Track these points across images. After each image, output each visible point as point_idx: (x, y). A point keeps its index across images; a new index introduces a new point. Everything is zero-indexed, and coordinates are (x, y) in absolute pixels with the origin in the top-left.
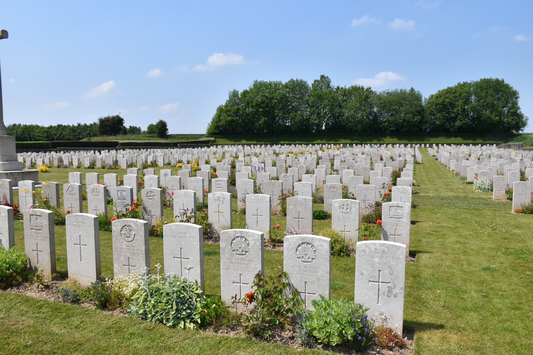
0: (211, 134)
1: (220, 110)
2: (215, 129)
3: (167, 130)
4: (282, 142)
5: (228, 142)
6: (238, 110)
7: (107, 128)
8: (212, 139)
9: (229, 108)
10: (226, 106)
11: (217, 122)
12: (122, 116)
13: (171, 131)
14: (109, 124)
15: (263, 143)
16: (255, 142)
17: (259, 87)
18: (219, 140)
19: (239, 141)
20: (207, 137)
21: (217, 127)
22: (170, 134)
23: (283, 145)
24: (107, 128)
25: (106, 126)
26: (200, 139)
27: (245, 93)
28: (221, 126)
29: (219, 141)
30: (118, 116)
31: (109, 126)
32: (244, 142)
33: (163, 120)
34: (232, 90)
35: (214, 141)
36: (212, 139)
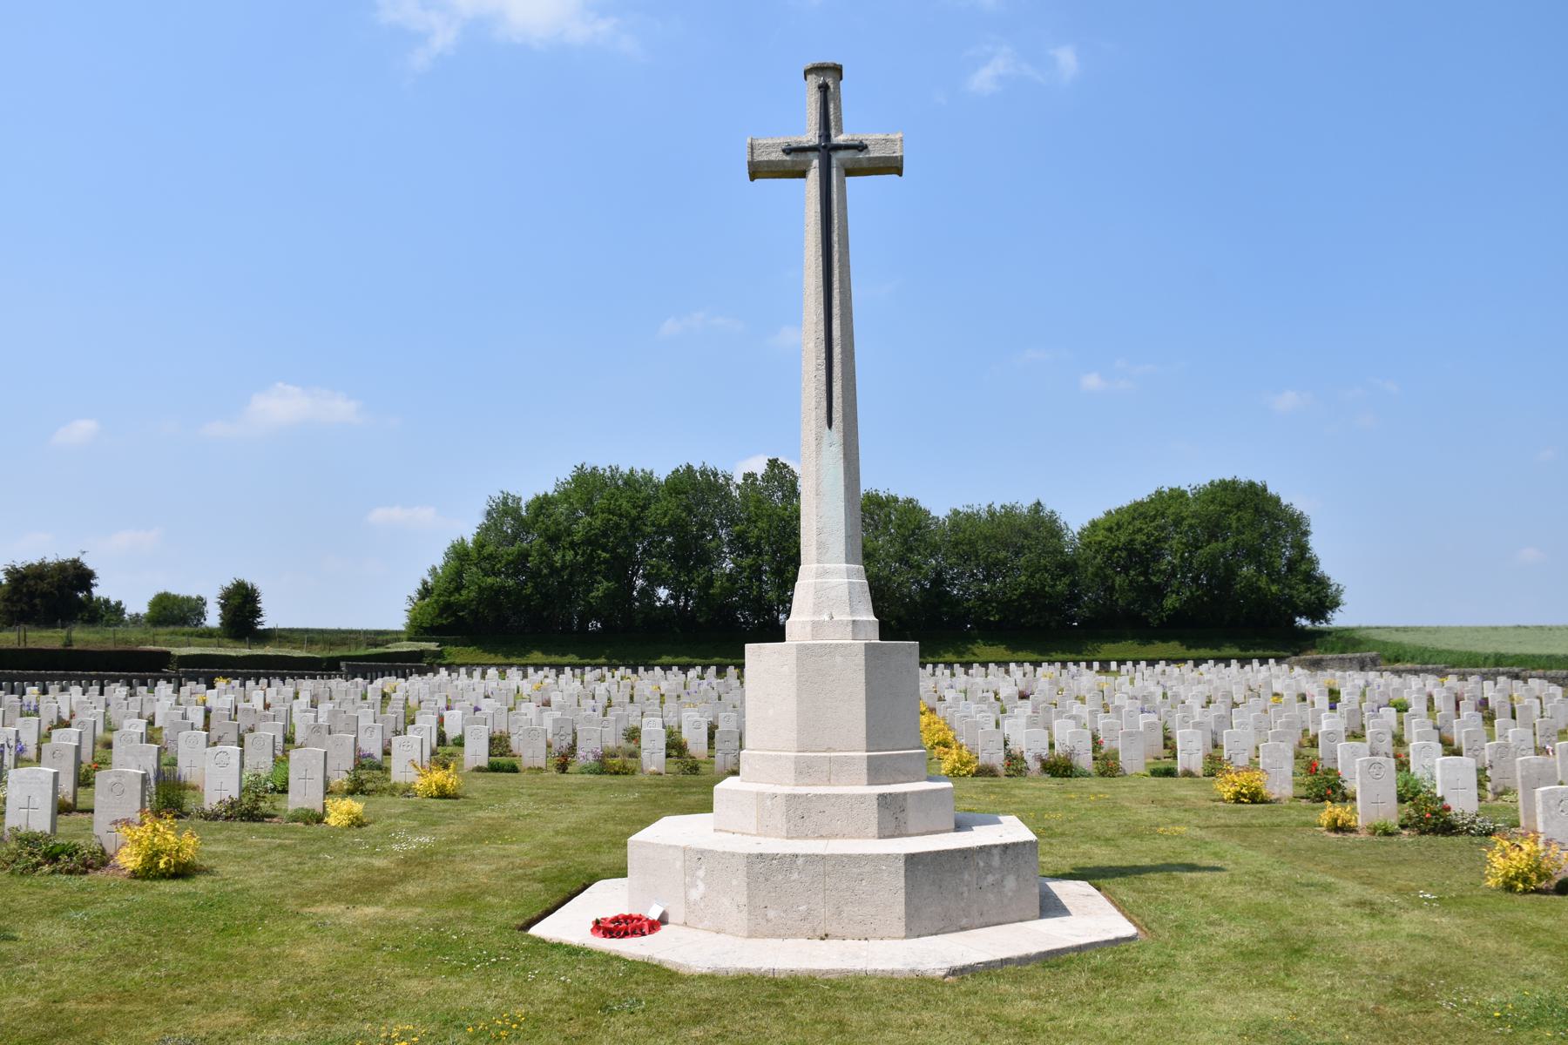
0: (419, 630)
1: (460, 555)
2: (440, 615)
3: (257, 613)
4: (666, 659)
5: (487, 658)
6: (524, 555)
7: (37, 601)
8: (432, 646)
9: (490, 549)
10: (480, 545)
11: (451, 594)
12: (89, 563)
13: (272, 616)
14: (44, 586)
15: (602, 660)
16: (573, 659)
17: (587, 484)
18: (454, 649)
19: (520, 655)
20: (410, 639)
21: (447, 608)
22: (266, 626)
23: (666, 668)
24: (37, 601)
25: (32, 595)
26: (393, 648)
27: (542, 505)
28: (463, 607)
29: (454, 652)
30: (75, 561)
31: (43, 595)
32: (537, 656)
33: (249, 580)
34: (497, 495)
35: (438, 655)
36: (432, 646)
